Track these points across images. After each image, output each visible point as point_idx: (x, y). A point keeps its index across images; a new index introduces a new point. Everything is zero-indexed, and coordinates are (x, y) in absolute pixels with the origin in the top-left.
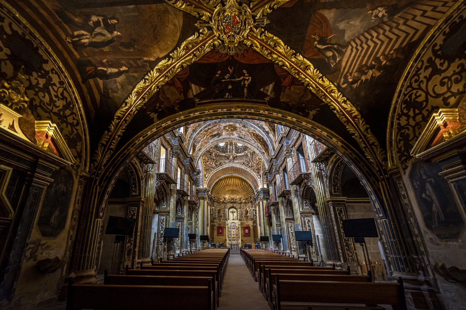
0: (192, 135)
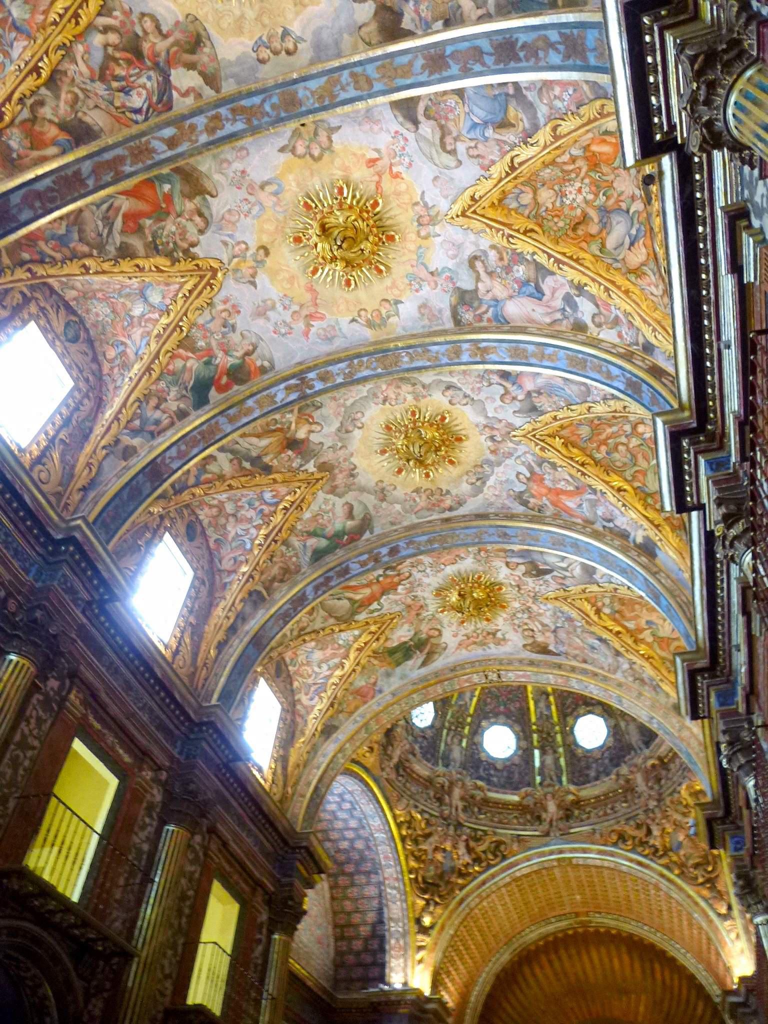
0: (242, 617)
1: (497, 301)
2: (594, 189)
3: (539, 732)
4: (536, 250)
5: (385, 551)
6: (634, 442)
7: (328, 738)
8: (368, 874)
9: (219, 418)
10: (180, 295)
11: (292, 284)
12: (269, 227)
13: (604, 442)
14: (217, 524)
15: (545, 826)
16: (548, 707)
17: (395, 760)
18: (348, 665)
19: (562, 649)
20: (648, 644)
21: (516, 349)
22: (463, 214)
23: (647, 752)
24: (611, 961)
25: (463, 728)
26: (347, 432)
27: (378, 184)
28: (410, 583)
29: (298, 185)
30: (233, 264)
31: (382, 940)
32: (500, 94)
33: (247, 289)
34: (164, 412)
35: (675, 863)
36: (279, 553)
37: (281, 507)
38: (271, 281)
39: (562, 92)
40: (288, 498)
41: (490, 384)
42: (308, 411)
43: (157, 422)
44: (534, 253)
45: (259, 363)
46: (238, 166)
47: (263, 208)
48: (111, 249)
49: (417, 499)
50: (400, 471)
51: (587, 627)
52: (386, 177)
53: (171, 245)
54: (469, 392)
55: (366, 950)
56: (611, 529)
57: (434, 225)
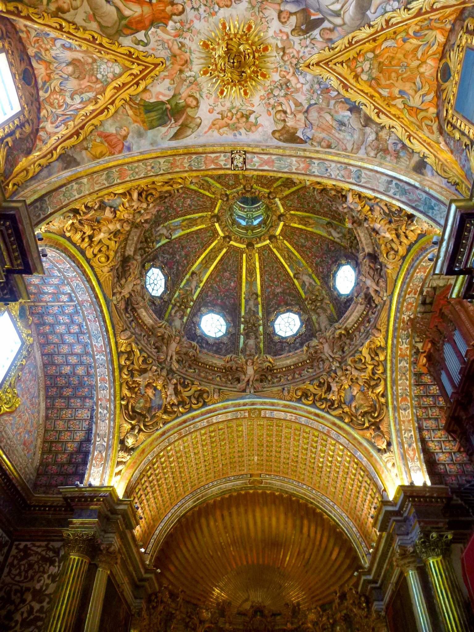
3: (246, 322)
7: (66, 168)
8: (85, 397)
15: (242, 385)
16: (256, 305)
17: (126, 292)
18: (103, 101)
19: (309, 134)
20: (399, 109)
23: (336, 325)
24: (270, 519)
25: (186, 308)
28: (181, 22)
31: (86, 454)
35: (347, 413)
51: (343, 92)
55: (70, 462)
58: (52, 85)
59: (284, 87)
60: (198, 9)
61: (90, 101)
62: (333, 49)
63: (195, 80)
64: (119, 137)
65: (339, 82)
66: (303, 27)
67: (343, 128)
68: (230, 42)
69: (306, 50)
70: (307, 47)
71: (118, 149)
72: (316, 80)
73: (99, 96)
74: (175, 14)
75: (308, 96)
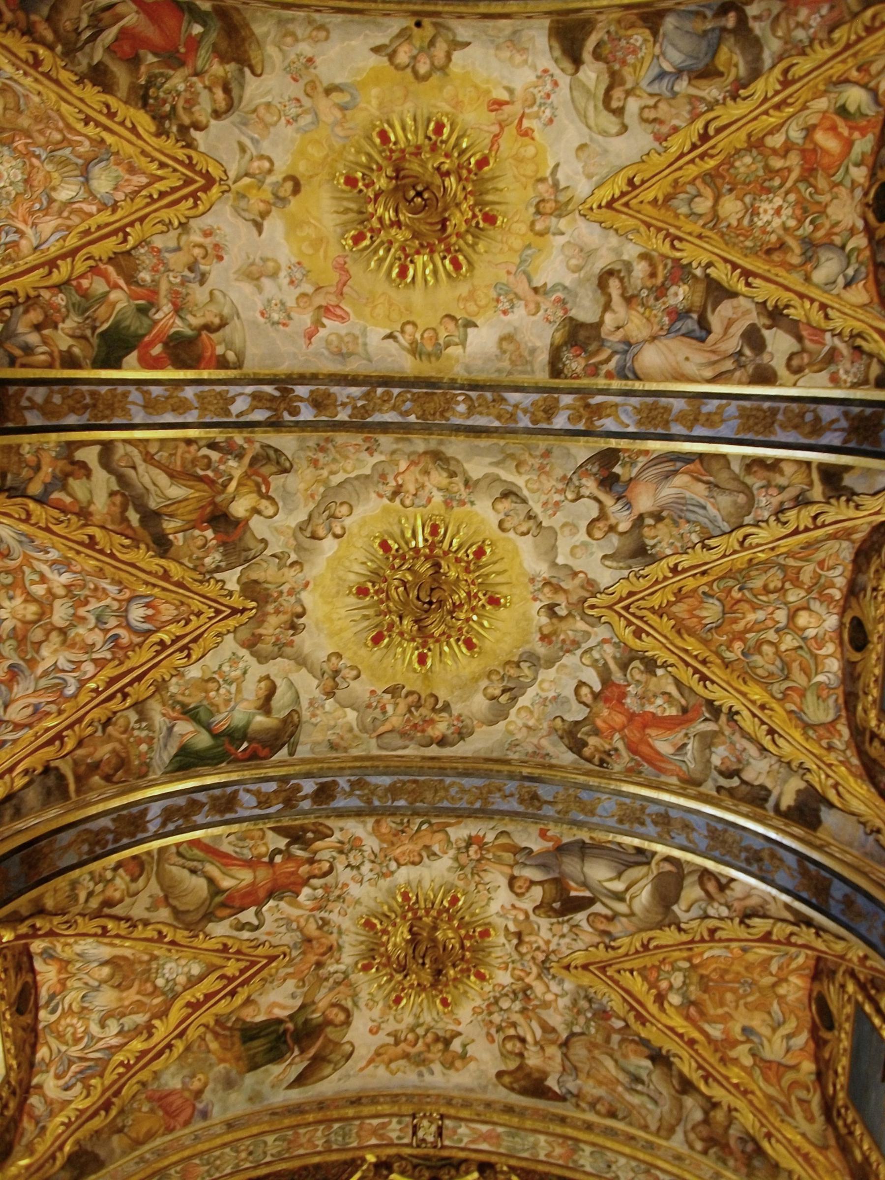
1: (629, 344)
2: (798, 212)
4: (715, 258)
5: (309, 786)
6: (789, 642)
9: (132, 388)
10: (144, 193)
11: (317, 250)
12: (317, 153)
13: (740, 636)
14: (25, 637)
18: (162, 1029)
19: (572, 1085)
20: (743, 1068)
21: (654, 407)
22: (609, 205)
26: (314, 537)
27: (496, 136)
28: (325, 887)
29: (381, 106)
30: (239, 184)
32: (713, 29)
33: (246, 230)
34: (45, 343)
36: (121, 722)
37: (155, 638)
38: (287, 237)
39: (808, 17)
40: (172, 628)
41: (579, 497)
42: (265, 470)
43: (28, 350)
44: (709, 265)
45: (220, 350)
46: (306, 49)
47: (317, 120)
48: (83, 62)
49: (390, 709)
50: (377, 639)
51: (636, 1026)
52: (511, 131)
53: (167, 107)
54: (537, 509)
56: (731, 792)
57: (560, 216)
58: (67, 1001)
59: (521, 996)
60: (358, 868)
61: (137, 1031)
62: (613, 948)
63: (346, 977)
64: (187, 1094)
65: (627, 1008)
66: (556, 905)
67: (640, 1087)
68: (418, 923)
69: (564, 941)
70: (563, 936)
71: (182, 1119)
72: (582, 994)
73: (156, 1022)
74: (314, 877)
75: (568, 1018)
